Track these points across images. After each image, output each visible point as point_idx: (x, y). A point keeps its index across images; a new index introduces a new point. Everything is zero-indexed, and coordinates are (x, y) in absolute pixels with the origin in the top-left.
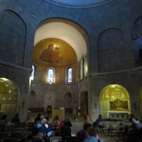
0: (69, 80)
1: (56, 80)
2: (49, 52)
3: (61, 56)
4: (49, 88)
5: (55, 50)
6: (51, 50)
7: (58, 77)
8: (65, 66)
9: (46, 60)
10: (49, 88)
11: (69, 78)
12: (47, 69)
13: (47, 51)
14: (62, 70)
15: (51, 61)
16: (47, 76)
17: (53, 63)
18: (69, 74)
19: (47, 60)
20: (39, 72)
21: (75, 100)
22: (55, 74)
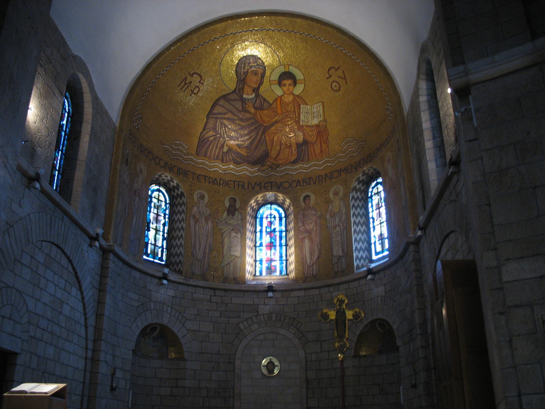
0: (379, 249)
1: (301, 261)
2: (245, 110)
3: (315, 122)
4: (264, 309)
5: (279, 92)
6: (256, 90)
7: (311, 241)
8: (345, 170)
9: (237, 153)
10: (264, 309)
11: (375, 234)
12: (246, 203)
13: (238, 105)
14: (331, 196)
15: (266, 155)
16: (249, 243)
17: (275, 167)
18: (373, 213)
19: (243, 152)
20: (197, 221)
21: (332, 315)
22: (292, 225)
